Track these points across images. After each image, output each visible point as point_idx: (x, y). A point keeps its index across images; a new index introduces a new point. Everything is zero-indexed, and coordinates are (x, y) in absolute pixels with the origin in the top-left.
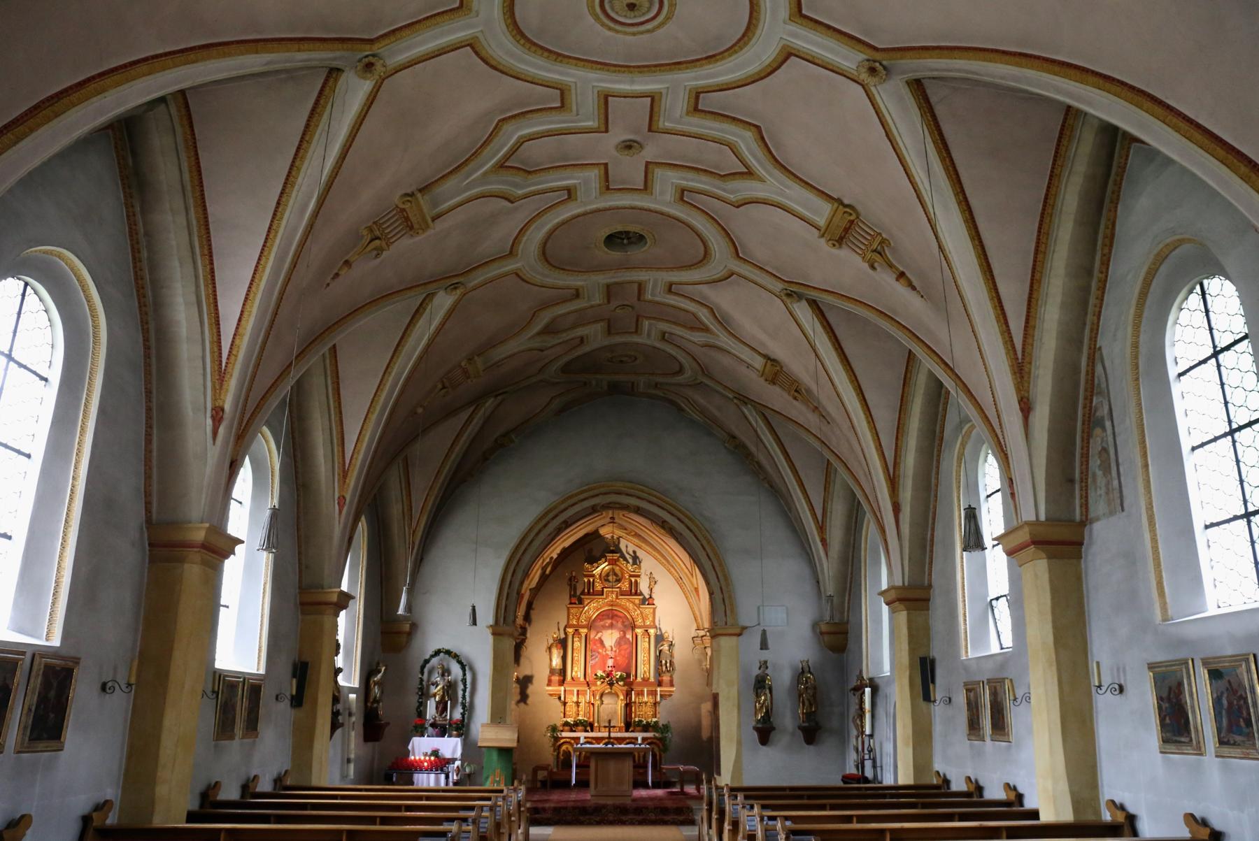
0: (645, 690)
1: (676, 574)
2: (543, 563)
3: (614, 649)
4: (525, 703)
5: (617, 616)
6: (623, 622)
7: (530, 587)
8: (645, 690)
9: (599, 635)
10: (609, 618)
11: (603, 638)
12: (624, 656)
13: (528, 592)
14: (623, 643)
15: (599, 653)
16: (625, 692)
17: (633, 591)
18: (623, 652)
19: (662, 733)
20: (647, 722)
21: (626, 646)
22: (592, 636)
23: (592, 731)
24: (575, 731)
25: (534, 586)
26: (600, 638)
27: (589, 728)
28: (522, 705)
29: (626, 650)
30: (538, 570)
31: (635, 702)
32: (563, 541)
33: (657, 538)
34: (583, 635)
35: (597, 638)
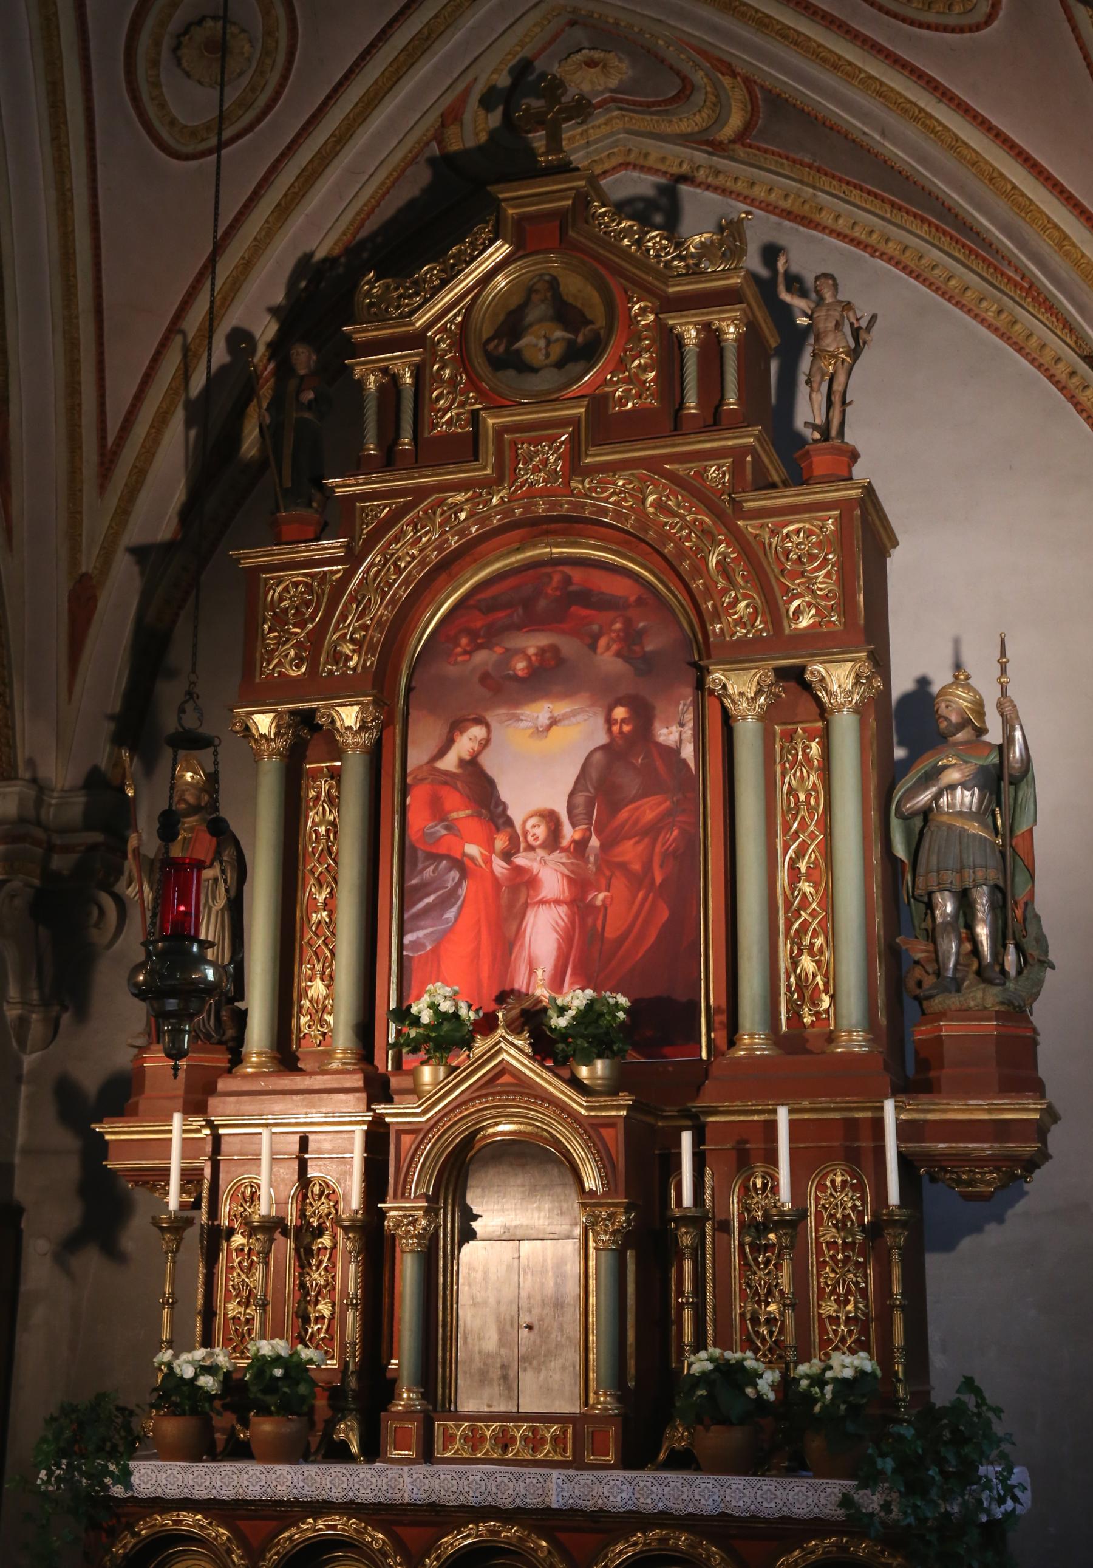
0: (783, 1116)
1: (1056, 345)
2: (186, 373)
3: (569, 833)
4: (113, 1252)
5: (586, 598)
6: (631, 638)
7: (134, 534)
8: (783, 1116)
9: (465, 744)
10: (532, 622)
11: (489, 763)
12: (639, 880)
13: (123, 567)
14: (630, 783)
15: (461, 865)
16: (615, 1139)
17: (692, 405)
18: (630, 851)
19: (915, 1487)
20: (786, 1384)
21: (650, 810)
22: (417, 757)
23: (372, 1451)
24: (240, 1451)
25: (165, 530)
26: (472, 766)
27: (349, 1433)
28: (91, 1260)
29: (653, 830)
30: (161, 420)
31: (696, 1221)
32: (284, 210)
33: (874, 68)
34: (354, 744)
35: (449, 763)
